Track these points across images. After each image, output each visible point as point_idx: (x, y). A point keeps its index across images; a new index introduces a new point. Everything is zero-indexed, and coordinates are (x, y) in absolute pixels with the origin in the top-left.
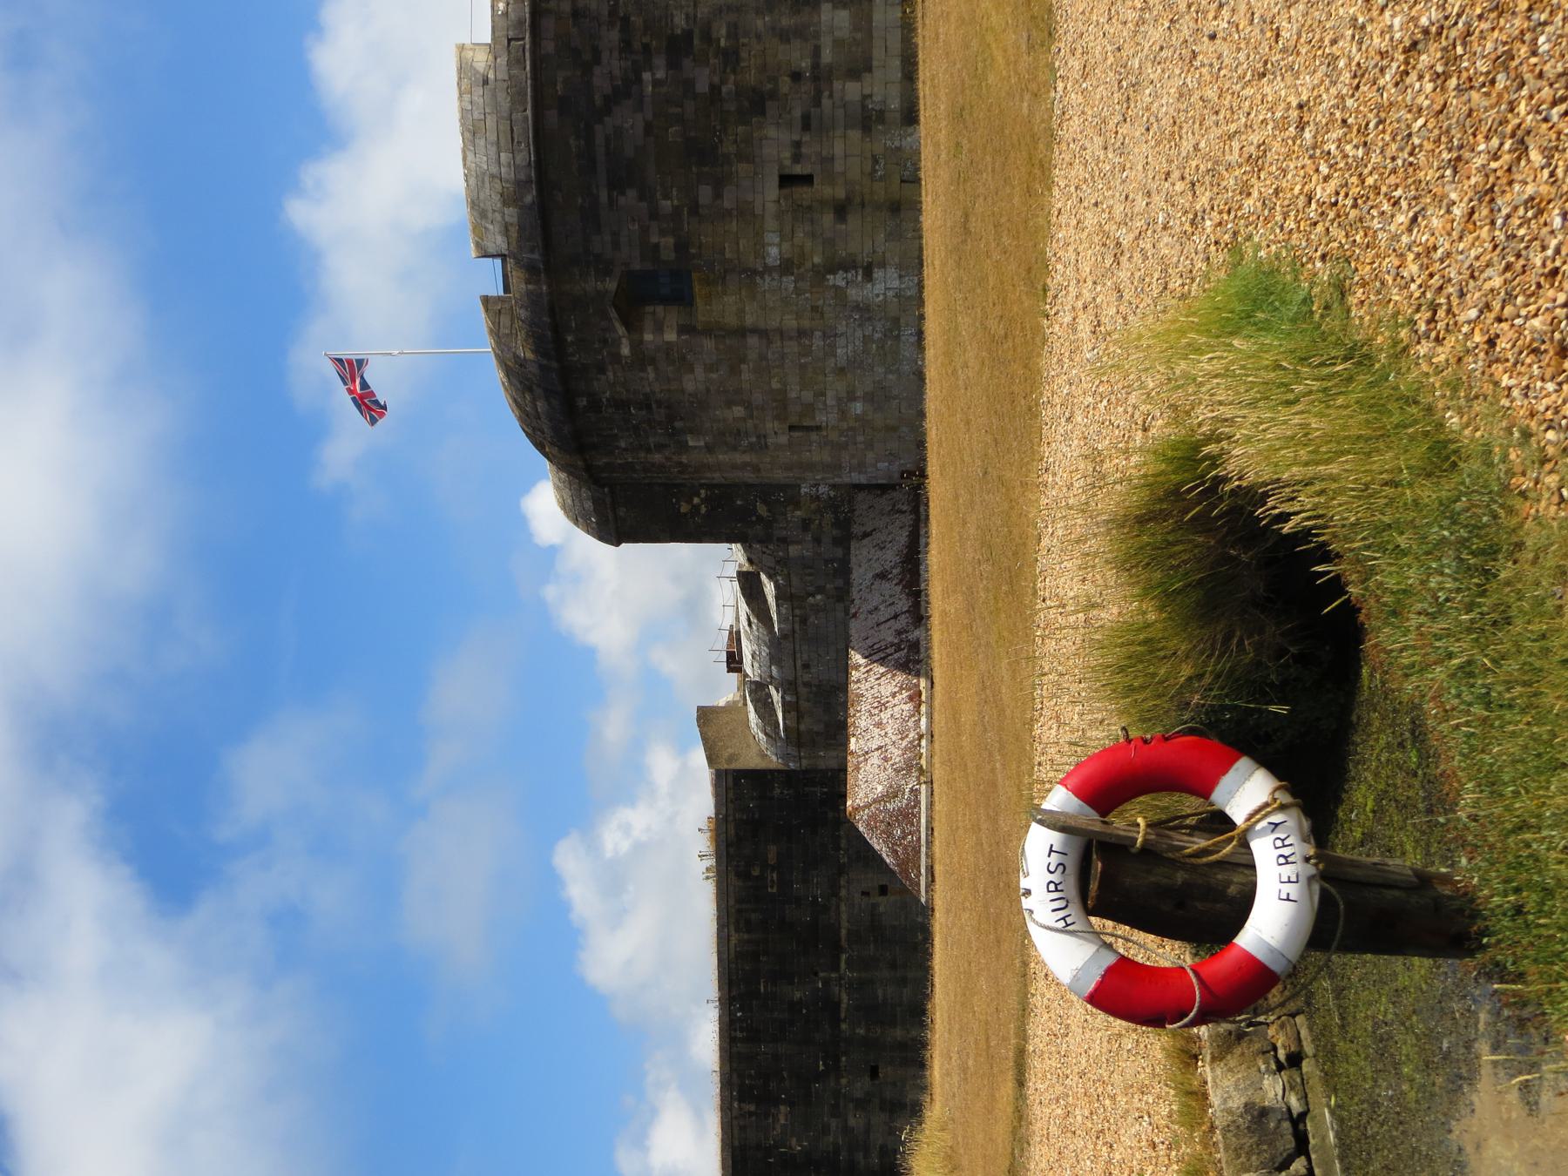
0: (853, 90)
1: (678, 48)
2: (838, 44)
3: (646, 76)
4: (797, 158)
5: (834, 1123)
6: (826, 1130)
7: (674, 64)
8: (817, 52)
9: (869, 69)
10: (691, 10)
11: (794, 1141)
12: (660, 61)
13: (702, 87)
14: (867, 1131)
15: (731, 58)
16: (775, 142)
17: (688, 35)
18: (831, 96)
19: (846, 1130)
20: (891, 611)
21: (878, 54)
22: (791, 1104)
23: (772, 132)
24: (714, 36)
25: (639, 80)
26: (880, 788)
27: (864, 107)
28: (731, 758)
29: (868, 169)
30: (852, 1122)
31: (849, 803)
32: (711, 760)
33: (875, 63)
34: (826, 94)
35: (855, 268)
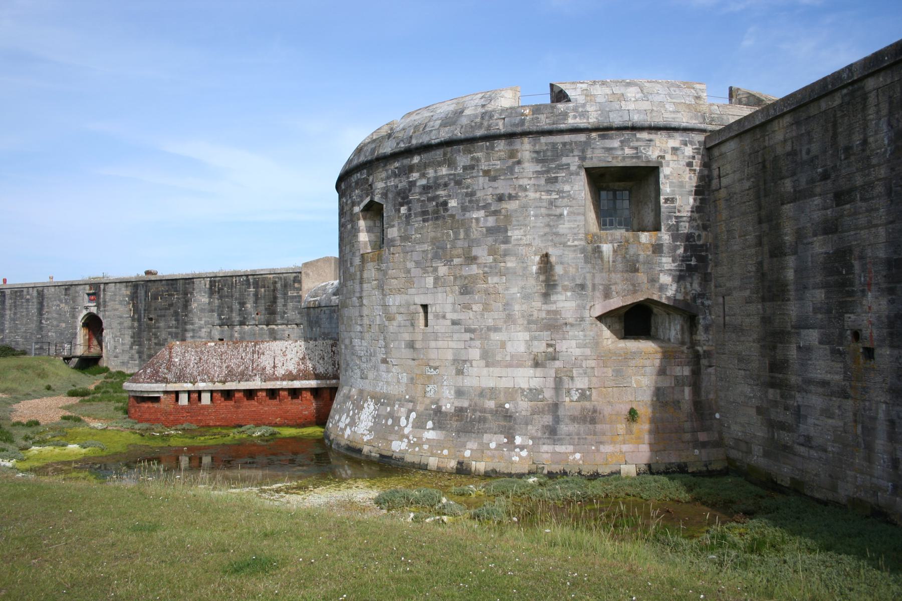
0: (475, 354)
1: (499, 232)
2: (503, 345)
3: (481, 214)
4: (437, 316)
5: (203, 322)
6: (200, 319)
7: (490, 231)
8: (496, 329)
9: (487, 366)
10: (524, 242)
11: (196, 305)
12: (491, 221)
13: (476, 251)
14: (200, 337)
15: (493, 270)
16: (444, 302)
17: (506, 241)
18: (471, 339)
19: (200, 328)
20: (280, 365)
21: (496, 371)
22: (209, 303)
23: (450, 299)
24: (507, 258)
25: (478, 209)
26: (176, 360)
27: (465, 361)
28: (307, 275)
29: (432, 364)
30: (204, 330)
31: (178, 343)
32: (306, 265)
33: (491, 369)
34: (473, 336)
35: (386, 353)
